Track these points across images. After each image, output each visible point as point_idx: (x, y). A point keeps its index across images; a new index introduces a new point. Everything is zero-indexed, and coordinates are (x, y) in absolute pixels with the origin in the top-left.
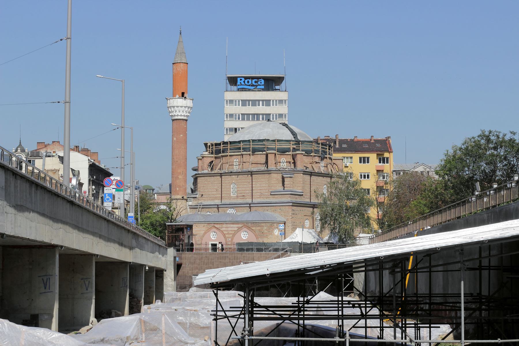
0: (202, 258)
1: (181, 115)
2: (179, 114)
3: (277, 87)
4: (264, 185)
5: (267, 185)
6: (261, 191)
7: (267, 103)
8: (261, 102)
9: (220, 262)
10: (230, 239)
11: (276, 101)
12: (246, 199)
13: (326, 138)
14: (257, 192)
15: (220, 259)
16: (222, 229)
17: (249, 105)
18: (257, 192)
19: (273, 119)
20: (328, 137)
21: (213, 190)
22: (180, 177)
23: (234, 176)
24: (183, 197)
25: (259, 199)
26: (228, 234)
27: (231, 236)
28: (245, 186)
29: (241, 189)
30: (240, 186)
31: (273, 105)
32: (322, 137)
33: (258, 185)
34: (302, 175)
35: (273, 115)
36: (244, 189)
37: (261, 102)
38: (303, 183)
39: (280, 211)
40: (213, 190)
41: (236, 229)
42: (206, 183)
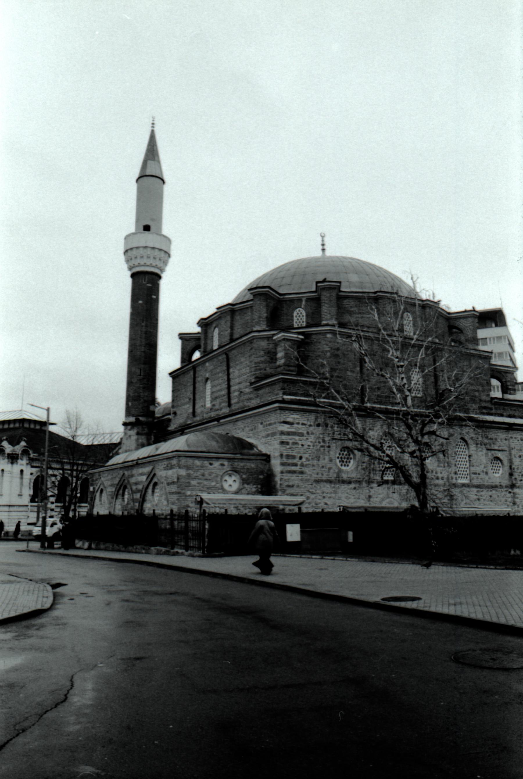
31: (490, 343)
36: (219, 388)
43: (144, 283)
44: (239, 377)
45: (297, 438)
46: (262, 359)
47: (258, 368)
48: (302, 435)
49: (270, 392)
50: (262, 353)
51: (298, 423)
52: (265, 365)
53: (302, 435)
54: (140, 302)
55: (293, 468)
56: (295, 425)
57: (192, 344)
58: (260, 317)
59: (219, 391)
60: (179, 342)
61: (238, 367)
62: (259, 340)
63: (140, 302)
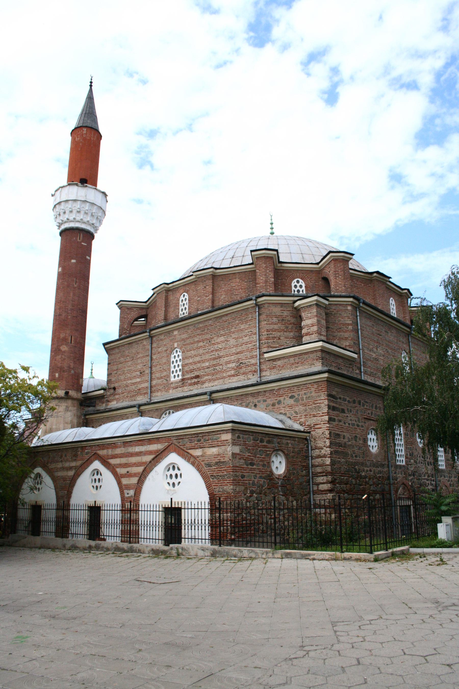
1: (74, 220)
2: (71, 218)
4: (246, 339)
6: (240, 356)
10: (132, 492)
12: (203, 383)
14: (229, 362)
16: (113, 461)
18: (229, 362)
21: (134, 374)
22: (64, 348)
23: (176, 333)
24: (67, 393)
25: (236, 379)
26: (129, 475)
27: (134, 480)
28: (201, 351)
29: (191, 361)
30: (189, 354)
33: (232, 342)
34: (349, 308)
36: (198, 359)
39: (291, 402)
40: (134, 374)
41: (148, 458)
43: (78, 240)
44: (236, 346)
46: (276, 327)
47: (271, 336)
48: (343, 411)
49: (298, 363)
51: (340, 398)
52: (279, 334)
57: (134, 314)
58: (266, 282)
59: (199, 362)
60: (118, 311)
61: (233, 336)
62: (271, 305)
63: (73, 261)
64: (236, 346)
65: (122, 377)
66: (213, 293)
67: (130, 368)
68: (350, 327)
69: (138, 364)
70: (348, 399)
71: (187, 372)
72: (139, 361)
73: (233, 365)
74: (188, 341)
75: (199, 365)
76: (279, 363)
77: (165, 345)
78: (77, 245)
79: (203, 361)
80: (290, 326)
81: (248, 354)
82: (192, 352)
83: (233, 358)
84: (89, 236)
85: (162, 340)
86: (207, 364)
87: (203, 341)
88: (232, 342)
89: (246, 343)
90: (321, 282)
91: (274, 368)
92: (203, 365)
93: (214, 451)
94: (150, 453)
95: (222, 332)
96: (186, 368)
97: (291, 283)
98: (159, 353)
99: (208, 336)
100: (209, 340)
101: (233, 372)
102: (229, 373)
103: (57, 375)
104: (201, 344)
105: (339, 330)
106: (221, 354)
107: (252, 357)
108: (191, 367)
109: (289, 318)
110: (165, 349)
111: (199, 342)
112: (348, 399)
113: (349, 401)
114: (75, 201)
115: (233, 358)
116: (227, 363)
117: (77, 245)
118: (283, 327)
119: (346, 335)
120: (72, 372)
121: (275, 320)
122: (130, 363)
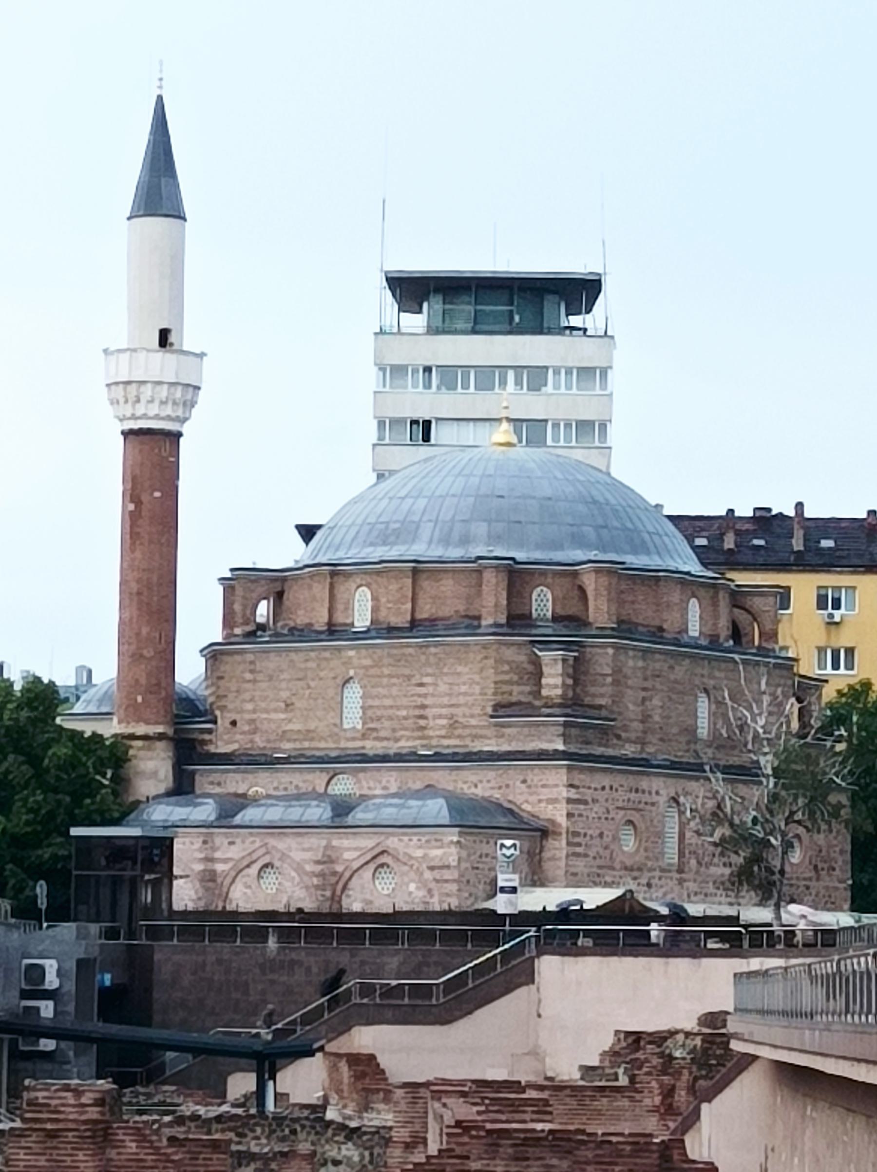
0: (204, 964)
3: (575, 321)
4: (464, 688)
5: (477, 689)
7: (535, 377)
8: (511, 375)
9: (273, 982)
11: (569, 371)
13: (758, 514)
14: (440, 717)
15: (272, 971)
17: (465, 386)
18: (440, 717)
19: (556, 439)
20: (769, 510)
23: (352, 653)
28: (394, 691)
29: (376, 703)
30: (374, 691)
32: (745, 511)
33: (443, 688)
34: (610, 651)
35: (556, 425)
36: (388, 702)
37: (511, 375)
38: (616, 683)
40: (273, 705)
42: (248, 676)
45: (582, 807)
46: (506, 677)
48: (585, 803)
50: (506, 668)
53: (585, 803)
54: (157, 494)
55: (578, 850)
56: (581, 790)
58: (496, 605)
59: (391, 707)
61: (446, 679)
63: (157, 494)
64: (450, 695)
65: (249, 706)
66: (414, 600)
67: (265, 694)
68: (609, 680)
69: (281, 690)
70: (593, 786)
71: (372, 720)
72: (284, 685)
73: (444, 722)
74: (372, 671)
75: (390, 712)
76: (508, 731)
77: (332, 669)
78: (153, 457)
79: (398, 708)
80: (526, 677)
81: (468, 712)
82: (380, 690)
83: (444, 711)
84: (175, 437)
85: (326, 659)
86: (404, 713)
87: (398, 677)
88: (443, 688)
89: (465, 694)
90: (576, 592)
91: (503, 736)
92: (399, 713)
93: (439, 852)
94: (356, 849)
95: (430, 670)
96: (370, 713)
97: (532, 592)
98: (321, 679)
99: (407, 672)
100: (409, 677)
101: (443, 732)
102: (438, 733)
103: (139, 699)
104: (394, 680)
105: (594, 683)
106: (426, 702)
107: (472, 716)
108: (379, 713)
109: (526, 665)
110: (332, 675)
111: (390, 676)
112: (593, 786)
113: (596, 789)
114: (159, 383)
115: (444, 711)
116: (435, 717)
117: (153, 457)
118: (516, 678)
119: (602, 690)
120: (163, 693)
121: (506, 668)
122: (263, 685)
